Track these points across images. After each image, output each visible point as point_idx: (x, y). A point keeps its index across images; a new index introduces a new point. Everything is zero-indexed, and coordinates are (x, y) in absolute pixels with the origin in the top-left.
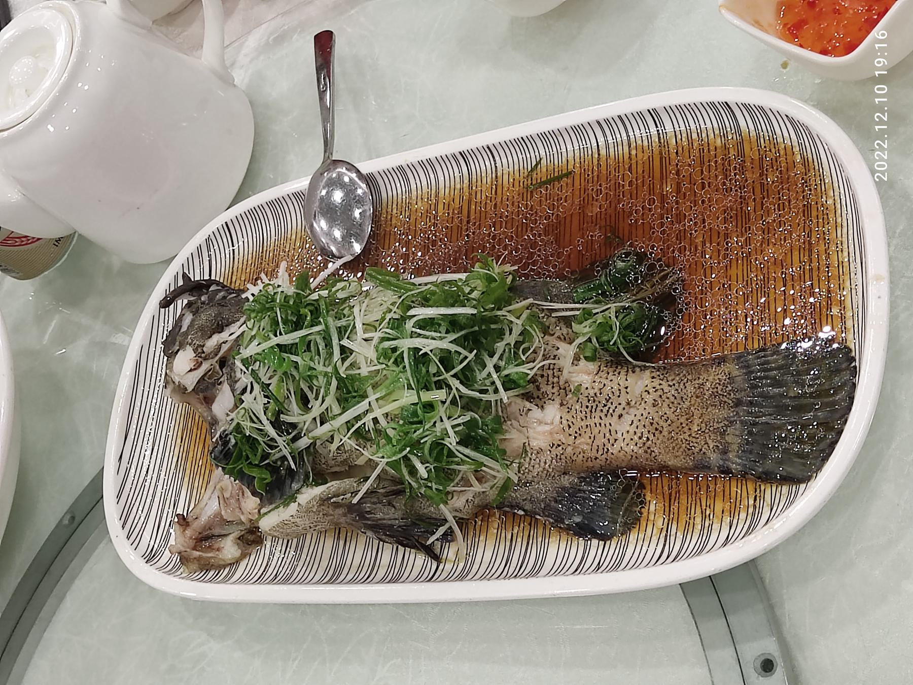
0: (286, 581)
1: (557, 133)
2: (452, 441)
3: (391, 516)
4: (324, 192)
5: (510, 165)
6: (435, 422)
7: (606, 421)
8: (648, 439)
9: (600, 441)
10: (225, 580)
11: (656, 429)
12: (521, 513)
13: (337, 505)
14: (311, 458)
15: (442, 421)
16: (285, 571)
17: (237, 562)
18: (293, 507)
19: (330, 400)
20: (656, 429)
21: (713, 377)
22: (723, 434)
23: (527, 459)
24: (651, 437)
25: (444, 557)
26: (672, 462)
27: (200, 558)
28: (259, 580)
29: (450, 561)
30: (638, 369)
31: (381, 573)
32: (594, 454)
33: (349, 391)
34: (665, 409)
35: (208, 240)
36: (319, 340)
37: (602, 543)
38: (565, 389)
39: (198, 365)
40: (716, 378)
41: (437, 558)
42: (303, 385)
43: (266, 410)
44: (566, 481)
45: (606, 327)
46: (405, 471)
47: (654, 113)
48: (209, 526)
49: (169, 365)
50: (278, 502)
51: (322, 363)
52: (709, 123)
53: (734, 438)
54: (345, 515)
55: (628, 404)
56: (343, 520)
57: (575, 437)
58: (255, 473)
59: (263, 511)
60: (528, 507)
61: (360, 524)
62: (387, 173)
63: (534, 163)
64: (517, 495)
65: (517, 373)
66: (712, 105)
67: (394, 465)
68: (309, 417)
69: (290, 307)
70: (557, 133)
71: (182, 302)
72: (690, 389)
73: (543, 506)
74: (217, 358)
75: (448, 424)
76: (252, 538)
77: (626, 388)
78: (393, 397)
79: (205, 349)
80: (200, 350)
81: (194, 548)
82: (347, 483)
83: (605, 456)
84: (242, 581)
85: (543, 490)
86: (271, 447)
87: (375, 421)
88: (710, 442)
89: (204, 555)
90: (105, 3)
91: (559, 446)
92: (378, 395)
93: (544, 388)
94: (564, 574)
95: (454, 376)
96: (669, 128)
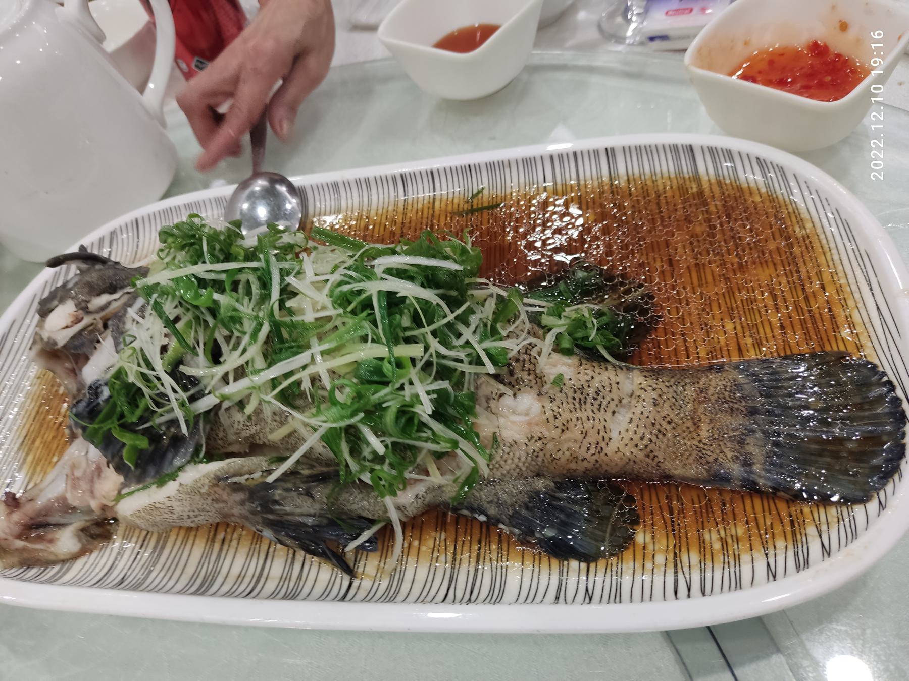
0: (136, 587)
1: (506, 164)
2: (425, 409)
3: (305, 510)
4: (245, 206)
5: (452, 191)
6: (403, 385)
7: (599, 415)
8: (651, 441)
9: (592, 438)
10: (51, 581)
11: (659, 431)
12: (482, 518)
13: (237, 488)
14: (208, 427)
15: (411, 383)
16: (137, 573)
17: (75, 557)
18: (171, 487)
19: (254, 351)
20: (659, 431)
21: (715, 383)
22: (742, 443)
23: (500, 451)
24: (654, 439)
25: (360, 570)
26: (677, 469)
27: (24, 549)
28: (99, 583)
29: (368, 576)
30: (624, 369)
31: (270, 586)
32: (582, 453)
33: (282, 341)
34: (666, 410)
35: (113, 234)
36: (253, 279)
37: (583, 565)
38: (541, 378)
39: (78, 320)
40: (720, 383)
41: (350, 571)
42: (220, 335)
43: (164, 349)
44: (540, 484)
45: (580, 324)
46: (345, 448)
47: (610, 153)
48: (47, 511)
49: (40, 325)
50: (149, 480)
51: (251, 306)
52: (665, 167)
53: (755, 449)
54: (242, 503)
55: (620, 401)
56: (237, 510)
57: (563, 431)
58: (127, 439)
59: (124, 492)
60: (492, 511)
61: (259, 518)
62: (320, 188)
63: (475, 191)
64: (483, 496)
65: (495, 347)
66: (675, 149)
67: (330, 438)
68: (219, 371)
69: (219, 241)
70: (506, 164)
71: (73, 270)
72: (691, 392)
73: (511, 512)
74: (103, 314)
75: (420, 389)
76: (100, 529)
77: (618, 383)
78: (343, 351)
79: (89, 305)
80: (83, 304)
81: (19, 537)
82: (258, 462)
83: (595, 457)
84: (76, 583)
85: (511, 492)
86: (158, 405)
87: (315, 379)
88: (726, 450)
89: (30, 546)
90: (62, 4)
91: (540, 439)
92: (326, 346)
93: (519, 374)
94: (528, 604)
95: (434, 334)
96: (622, 170)
